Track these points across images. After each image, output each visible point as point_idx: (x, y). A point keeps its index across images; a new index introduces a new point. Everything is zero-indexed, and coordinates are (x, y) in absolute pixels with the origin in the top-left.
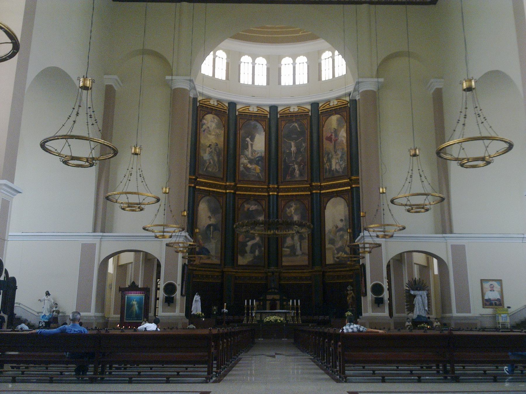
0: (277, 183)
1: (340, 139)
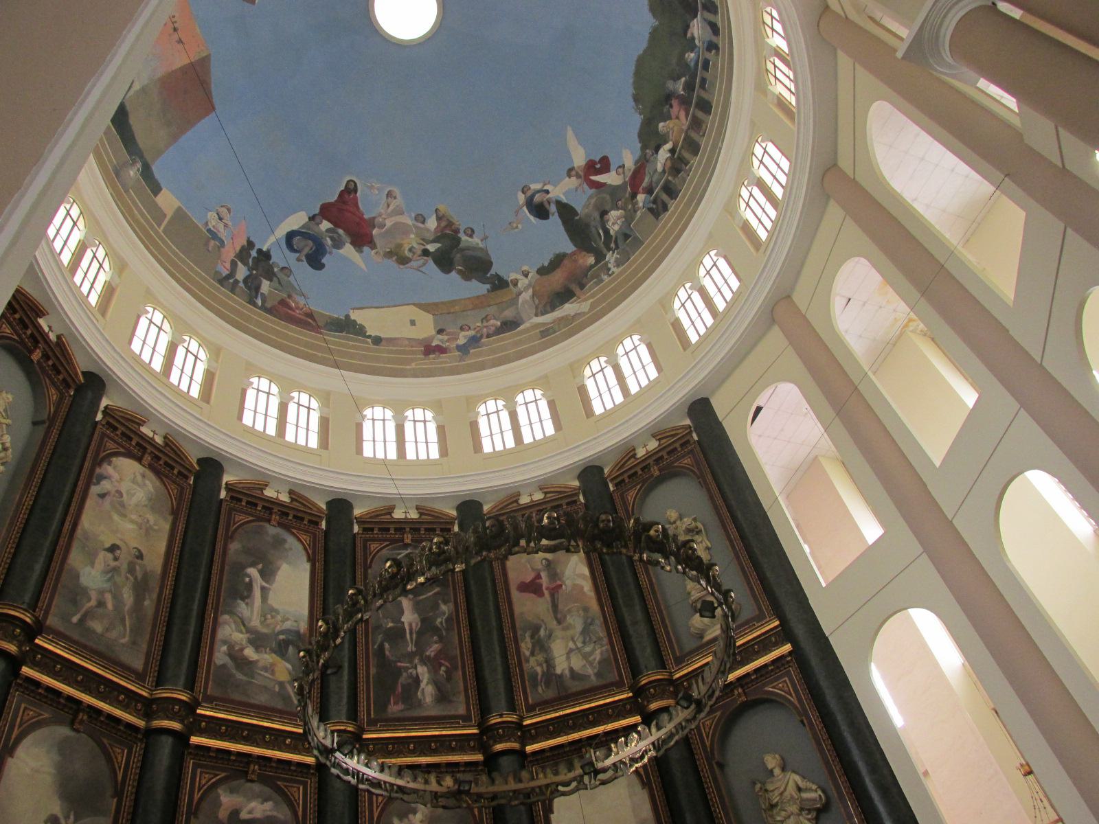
1: (568, 582)
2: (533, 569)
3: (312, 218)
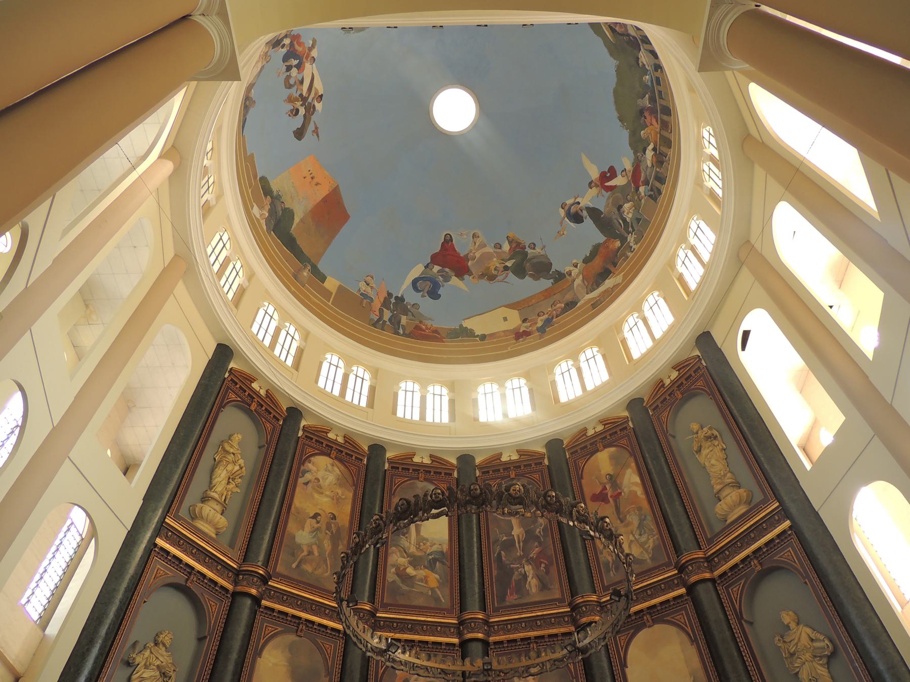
0: (484, 608)
1: (626, 490)
2: (601, 483)
3: (426, 267)
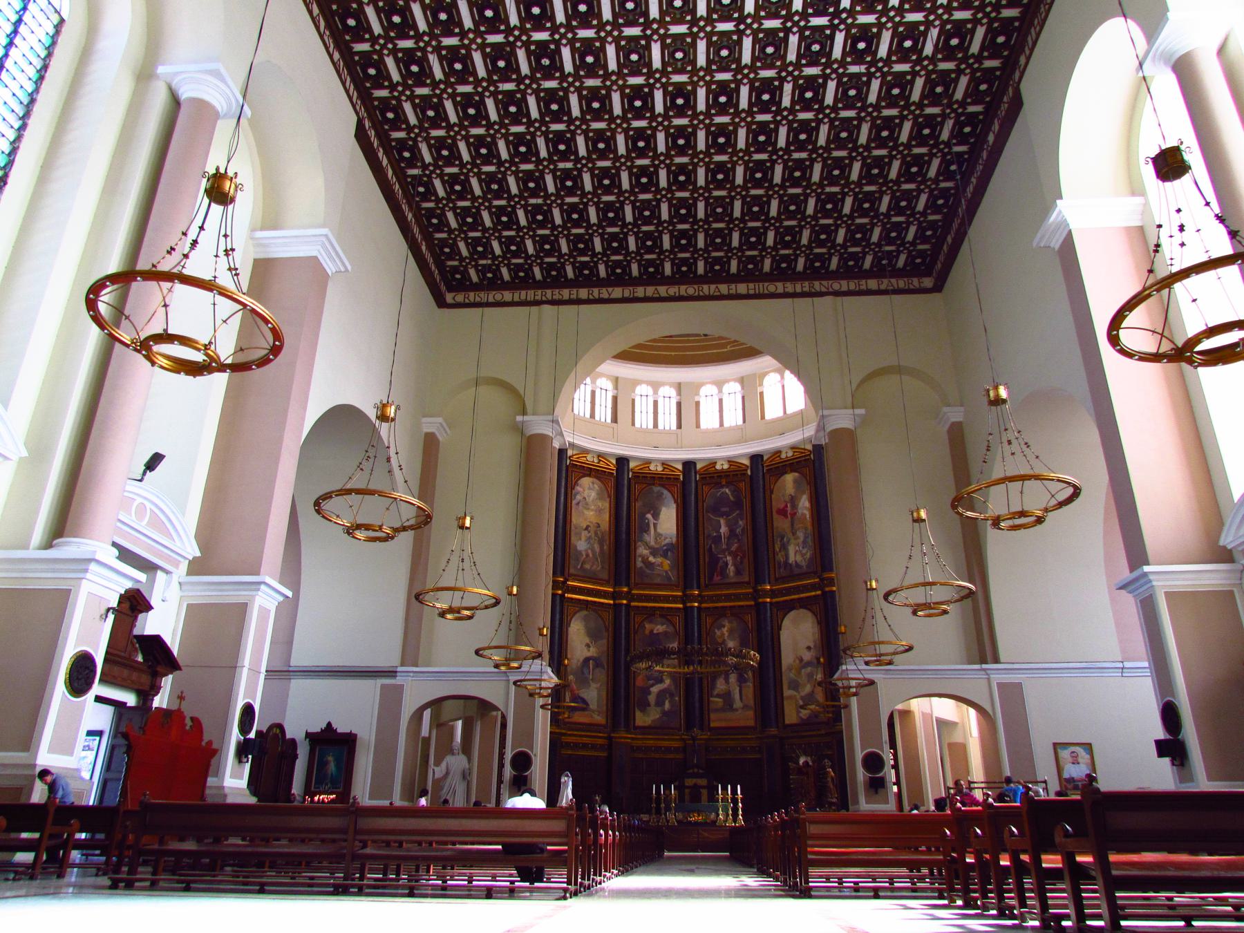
0: (699, 588)
1: (800, 511)
